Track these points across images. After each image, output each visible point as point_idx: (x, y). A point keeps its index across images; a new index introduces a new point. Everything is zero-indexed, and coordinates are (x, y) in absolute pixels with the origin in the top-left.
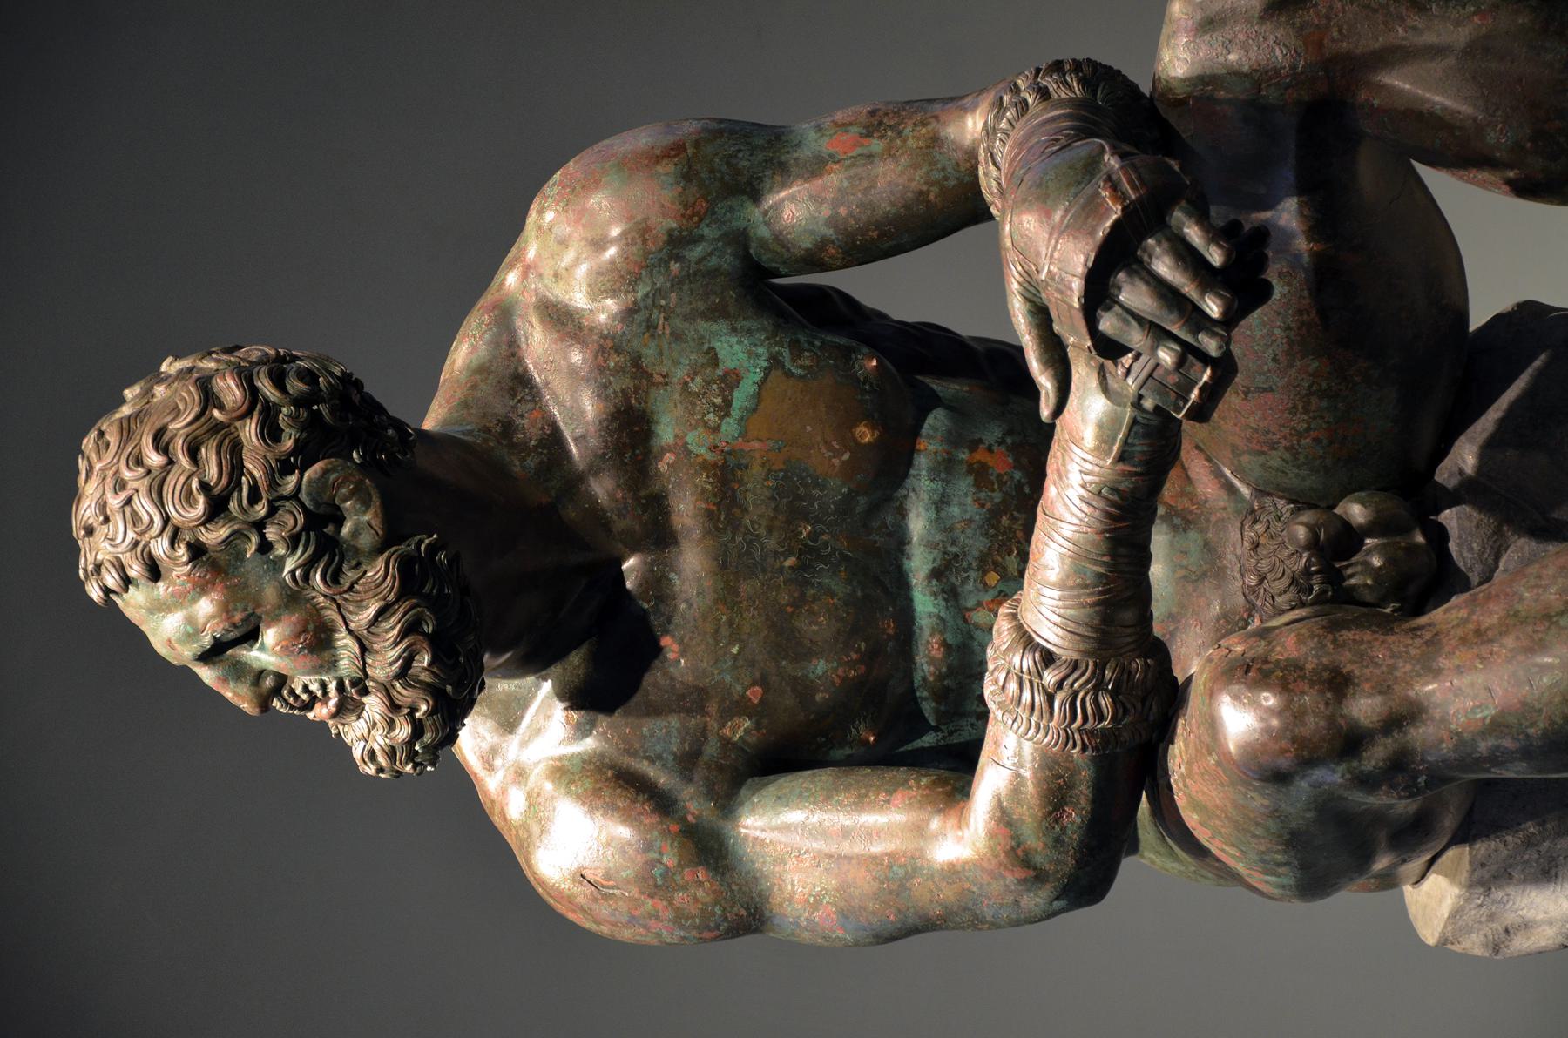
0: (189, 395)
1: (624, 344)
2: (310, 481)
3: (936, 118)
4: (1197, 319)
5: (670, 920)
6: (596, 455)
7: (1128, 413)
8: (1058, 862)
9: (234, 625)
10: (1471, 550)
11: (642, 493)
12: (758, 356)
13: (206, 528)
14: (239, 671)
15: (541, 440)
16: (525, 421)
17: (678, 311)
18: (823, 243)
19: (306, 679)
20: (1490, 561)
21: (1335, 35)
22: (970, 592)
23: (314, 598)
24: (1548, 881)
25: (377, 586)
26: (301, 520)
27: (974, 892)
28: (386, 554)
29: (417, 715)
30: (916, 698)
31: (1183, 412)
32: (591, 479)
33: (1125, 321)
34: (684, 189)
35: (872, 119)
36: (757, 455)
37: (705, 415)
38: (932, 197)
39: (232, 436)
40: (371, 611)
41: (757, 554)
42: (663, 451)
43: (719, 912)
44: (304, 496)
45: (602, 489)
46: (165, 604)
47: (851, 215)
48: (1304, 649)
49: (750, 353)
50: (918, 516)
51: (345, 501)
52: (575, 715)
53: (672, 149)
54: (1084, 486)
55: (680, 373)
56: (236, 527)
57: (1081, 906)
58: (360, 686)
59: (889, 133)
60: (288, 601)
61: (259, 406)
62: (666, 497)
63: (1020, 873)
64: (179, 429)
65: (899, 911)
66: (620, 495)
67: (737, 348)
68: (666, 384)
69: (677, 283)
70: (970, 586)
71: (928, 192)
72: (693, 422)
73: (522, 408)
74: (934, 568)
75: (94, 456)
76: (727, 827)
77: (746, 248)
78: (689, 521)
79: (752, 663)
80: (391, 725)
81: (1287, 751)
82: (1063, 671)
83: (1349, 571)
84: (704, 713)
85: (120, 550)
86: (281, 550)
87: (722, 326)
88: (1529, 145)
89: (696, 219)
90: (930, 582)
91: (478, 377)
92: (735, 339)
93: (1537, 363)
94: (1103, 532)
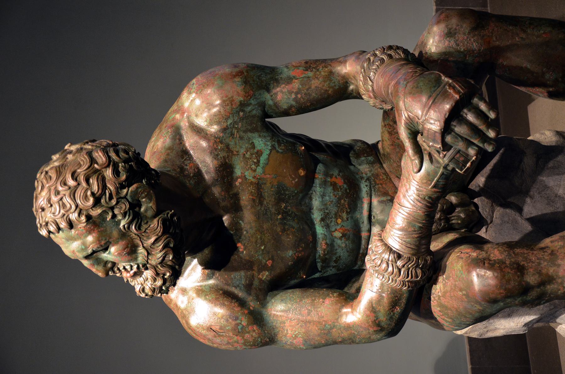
0: (84, 160)
1: (223, 141)
2: (132, 192)
3: (330, 65)
4: (485, 138)
6: (214, 179)
7: (441, 170)
8: (389, 324)
9: (101, 246)
10: (486, 211)
11: (231, 193)
12: (268, 145)
13: (92, 210)
14: (98, 261)
15: (194, 174)
16: (188, 167)
17: (241, 129)
18: (291, 107)
19: (124, 264)
20: (492, 214)
21: (494, 39)
22: (333, 226)
23: (131, 235)
24: (509, 317)
25: (154, 231)
26: (128, 206)
28: (157, 218)
29: (166, 277)
30: (316, 262)
31: (463, 171)
32: (213, 188)
33: (456, 138)
34: (245, 86)
35: (307, 65)
36: (269, 180)
37: (251, 166)
38: (330, 92)
39: (101, 175)
40: (152, 240)
41: (269, 214)
42: (237, 178)
43: (260, 340)
44: (129, 197)
45: (217, 191)
46: (74, 238)
47: (302, 97)
48: (503, 256)
49: (265, 144)
50: (316, 200)
51: (143, 198)
52: (207, 271)
53: (239, 73)
54: (419, 196)
55: (242, 151)
56: (104, 209)
57: (389, 337)
58: (145, 267)
59: (314, 70)
60: (122, 236)
61: (112, 163)
62: (238, 194)
63: (375, 328)
64: (81, 172)
65: (326, 340)
66: (223, 193)
67: (261, 142)
68: (238, 155)
69: (242, 119)
70: (333, 224)
71: (329, 90)
72: (247, 168)
73: (186, 162)
74: (322, 218)
75: (44, 181)
76: (264, 311)
77: (264, 107)
78: (246, 203)
79: (268, 253)
80: (155, 280)
81: (503, 293)
82: (406, 260)
83: (452, 218)
84: (253, 270)
85: (56, 217)
86: (120, 217)
87: (256, 135)
88: (560, 79)
89: (249, 97)
90: (321, 222)
91: (169, 151)
92: (260, 139)
93: (501, 151)
94: (425, 212)
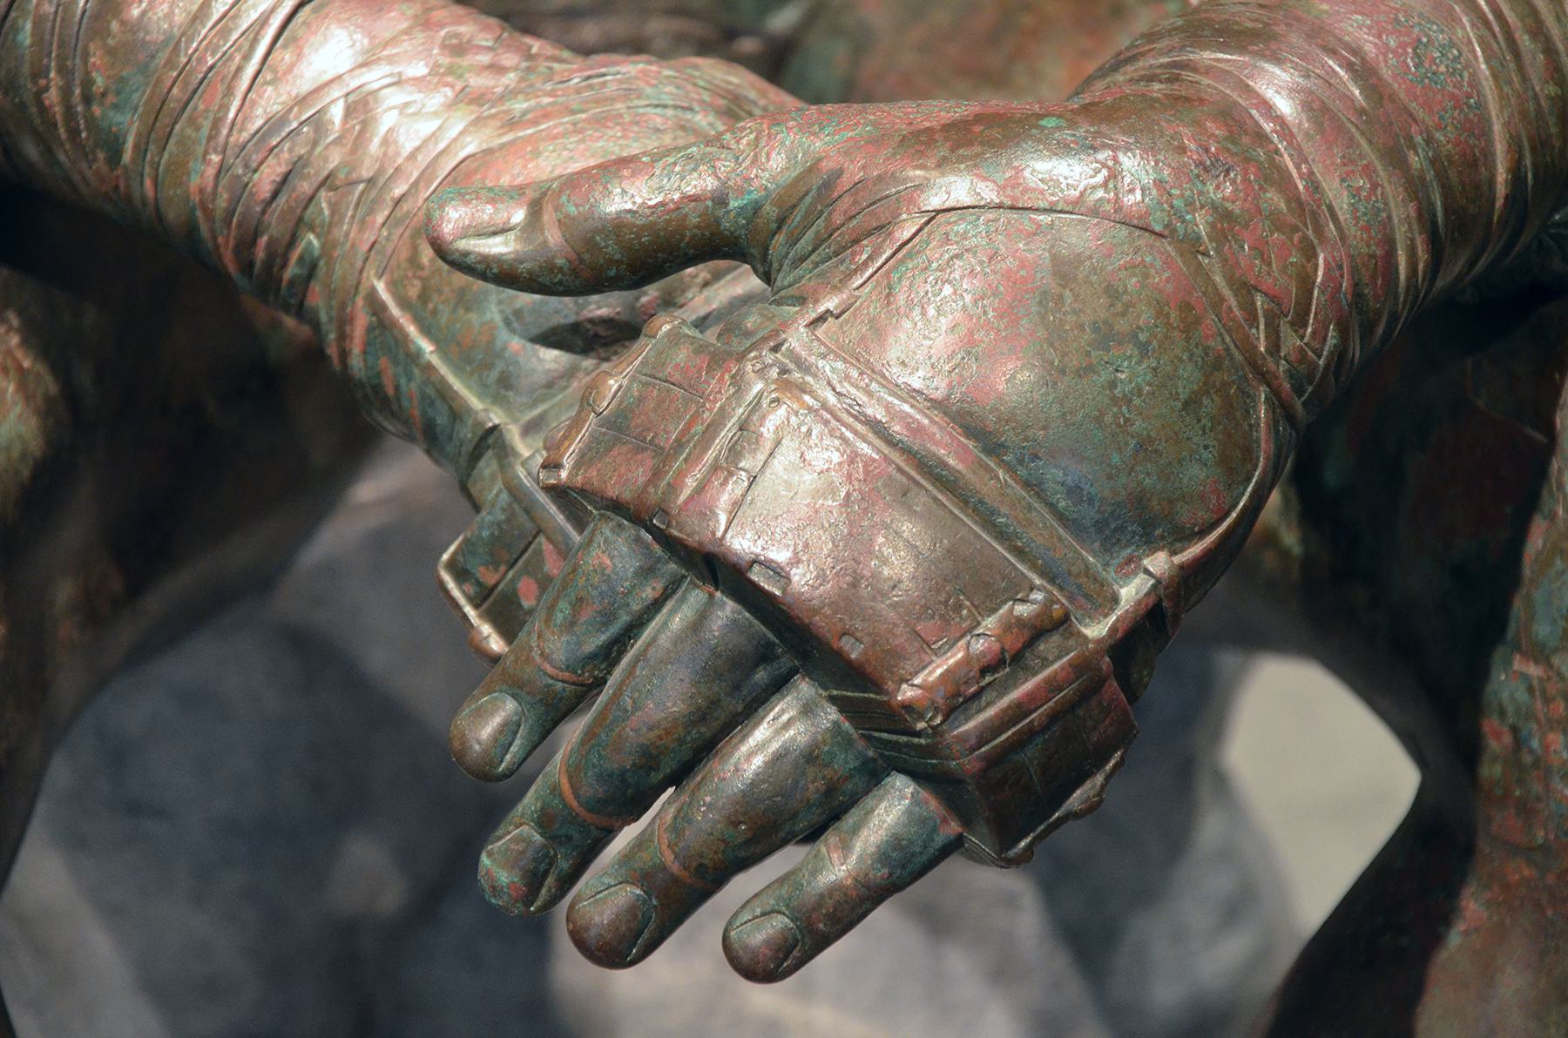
33: (608, 617)
54: (328, 181)
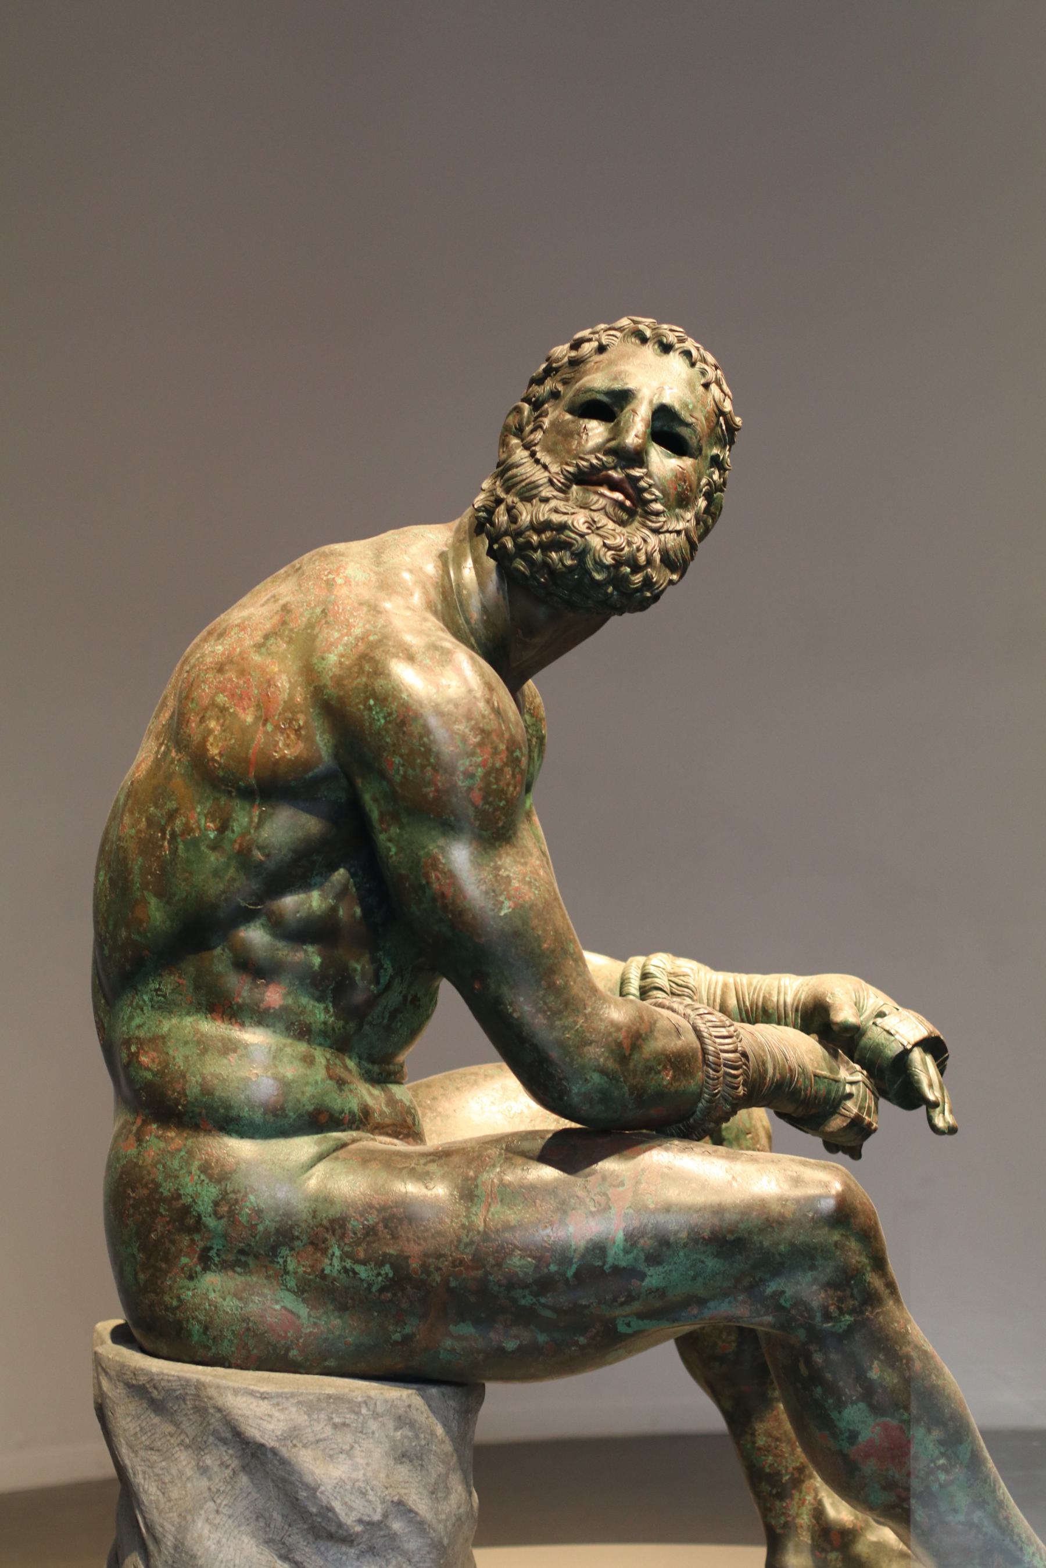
5: (493, 764)
27: (585, 1009)
63: (626, 1044)
65: (553, 951)
